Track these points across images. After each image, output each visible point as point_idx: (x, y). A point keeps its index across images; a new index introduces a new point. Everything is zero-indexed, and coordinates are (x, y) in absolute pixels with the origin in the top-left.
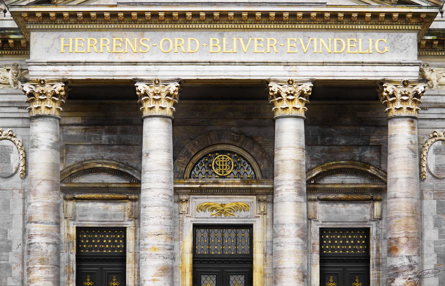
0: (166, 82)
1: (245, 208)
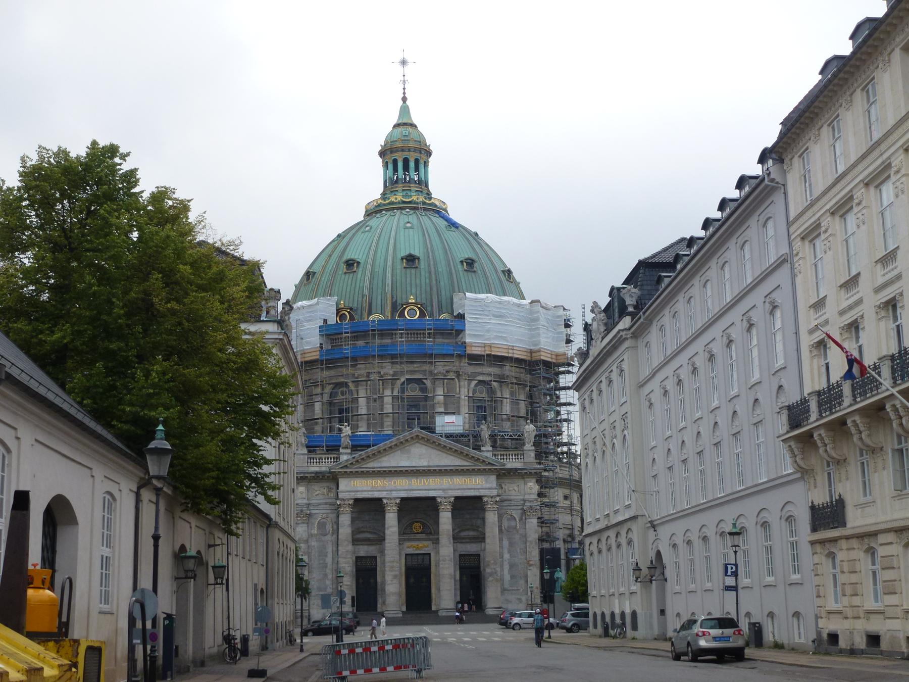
0: (395, 498)
1: (427, 547)
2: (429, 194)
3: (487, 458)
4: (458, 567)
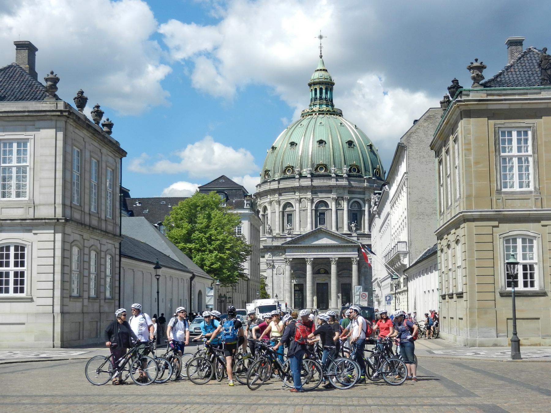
2: (332, 106)
3: (353, 240)
4: (341, 289)
